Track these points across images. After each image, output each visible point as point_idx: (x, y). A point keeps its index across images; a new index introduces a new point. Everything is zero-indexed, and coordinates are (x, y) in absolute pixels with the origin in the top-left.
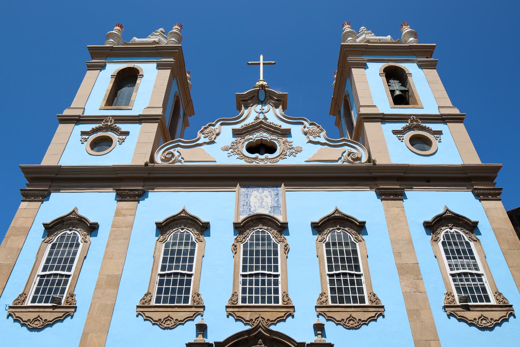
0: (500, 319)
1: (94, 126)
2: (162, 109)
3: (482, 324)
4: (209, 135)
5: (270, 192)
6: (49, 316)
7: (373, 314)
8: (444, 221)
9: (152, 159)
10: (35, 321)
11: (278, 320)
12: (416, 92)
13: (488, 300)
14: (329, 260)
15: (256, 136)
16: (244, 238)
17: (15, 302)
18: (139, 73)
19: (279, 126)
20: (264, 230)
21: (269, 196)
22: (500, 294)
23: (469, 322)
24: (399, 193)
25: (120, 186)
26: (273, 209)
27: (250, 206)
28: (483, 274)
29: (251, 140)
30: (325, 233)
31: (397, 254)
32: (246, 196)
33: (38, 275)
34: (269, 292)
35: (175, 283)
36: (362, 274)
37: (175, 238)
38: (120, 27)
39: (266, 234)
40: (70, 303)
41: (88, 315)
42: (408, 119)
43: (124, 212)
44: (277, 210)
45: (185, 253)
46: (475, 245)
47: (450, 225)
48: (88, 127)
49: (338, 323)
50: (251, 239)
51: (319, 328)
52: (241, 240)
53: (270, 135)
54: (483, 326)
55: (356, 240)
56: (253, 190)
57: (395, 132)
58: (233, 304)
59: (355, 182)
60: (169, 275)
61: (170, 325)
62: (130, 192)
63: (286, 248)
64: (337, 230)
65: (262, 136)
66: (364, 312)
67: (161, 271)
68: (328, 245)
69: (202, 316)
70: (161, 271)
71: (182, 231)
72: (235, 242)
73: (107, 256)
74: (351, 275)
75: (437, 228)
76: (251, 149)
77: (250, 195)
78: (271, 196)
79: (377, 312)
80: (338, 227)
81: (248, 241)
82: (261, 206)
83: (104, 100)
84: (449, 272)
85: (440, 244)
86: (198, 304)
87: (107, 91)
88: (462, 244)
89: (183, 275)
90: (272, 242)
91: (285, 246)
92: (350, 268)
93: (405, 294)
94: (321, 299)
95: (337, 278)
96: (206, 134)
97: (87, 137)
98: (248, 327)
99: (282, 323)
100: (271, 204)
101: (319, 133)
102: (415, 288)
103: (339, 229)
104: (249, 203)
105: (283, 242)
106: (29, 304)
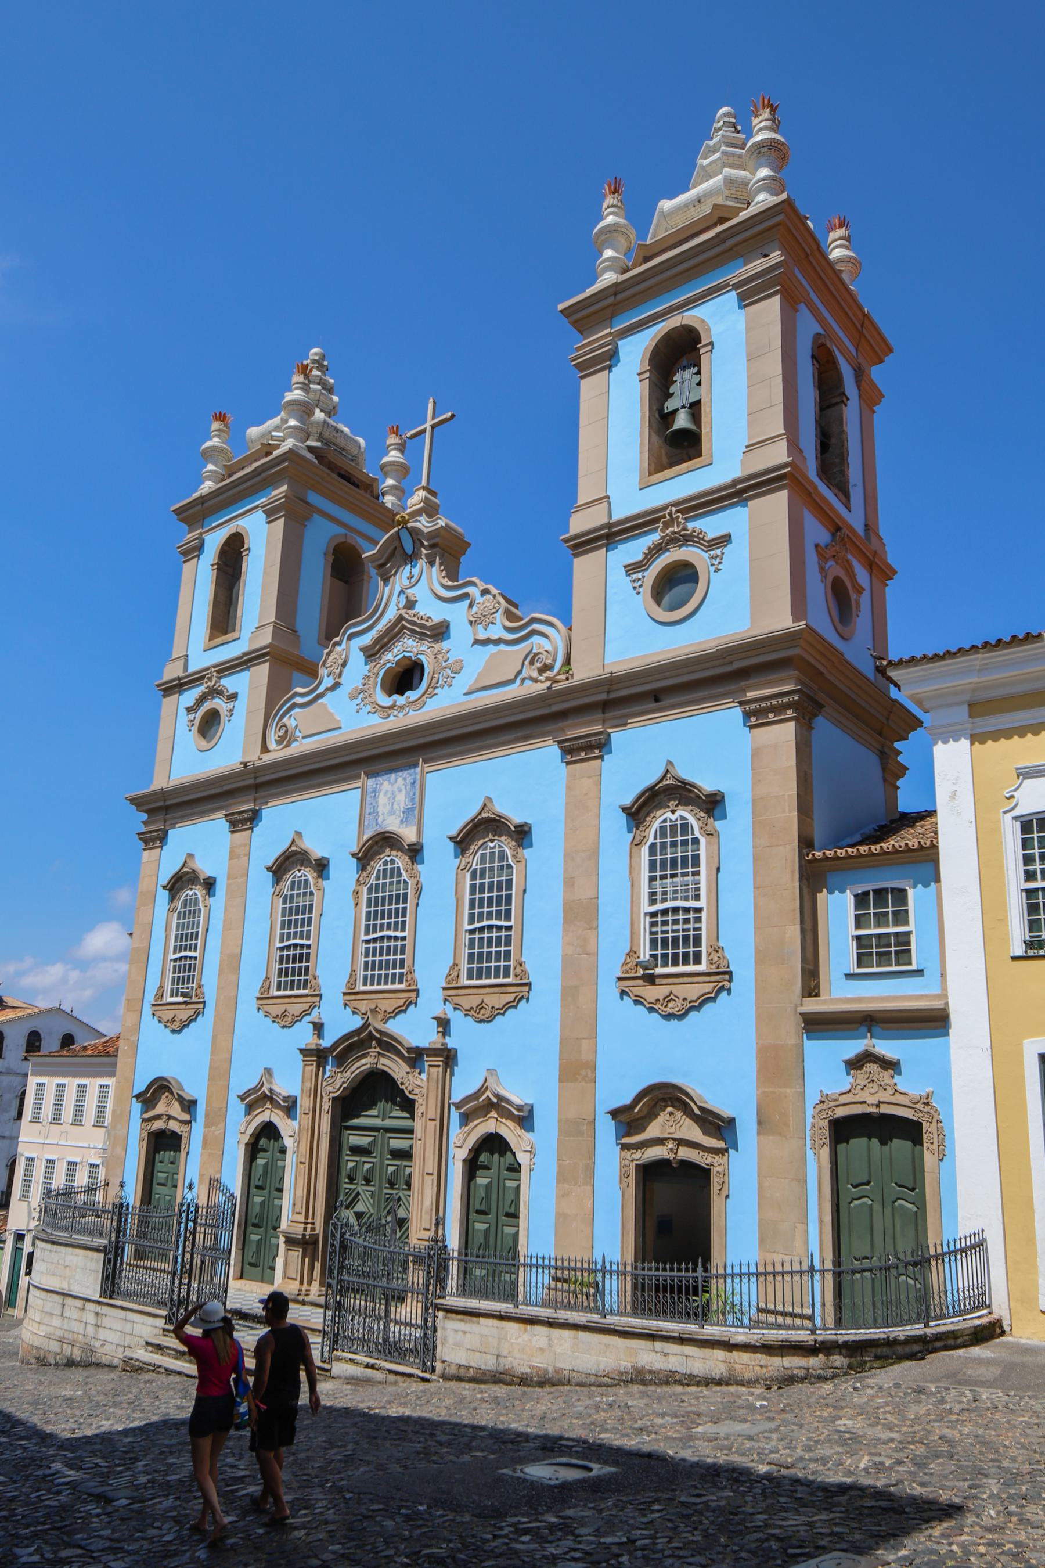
7: (511, 997)
8: (662, 796)
24: (594, 743)
31: (569, 882)
47: (672, 804)
51: (444, 1024)
59: (527, 732)
75: (647, 815)
80: (491, 836)
85: (645, 850)
93: (565, 957)
103: (492, 841)
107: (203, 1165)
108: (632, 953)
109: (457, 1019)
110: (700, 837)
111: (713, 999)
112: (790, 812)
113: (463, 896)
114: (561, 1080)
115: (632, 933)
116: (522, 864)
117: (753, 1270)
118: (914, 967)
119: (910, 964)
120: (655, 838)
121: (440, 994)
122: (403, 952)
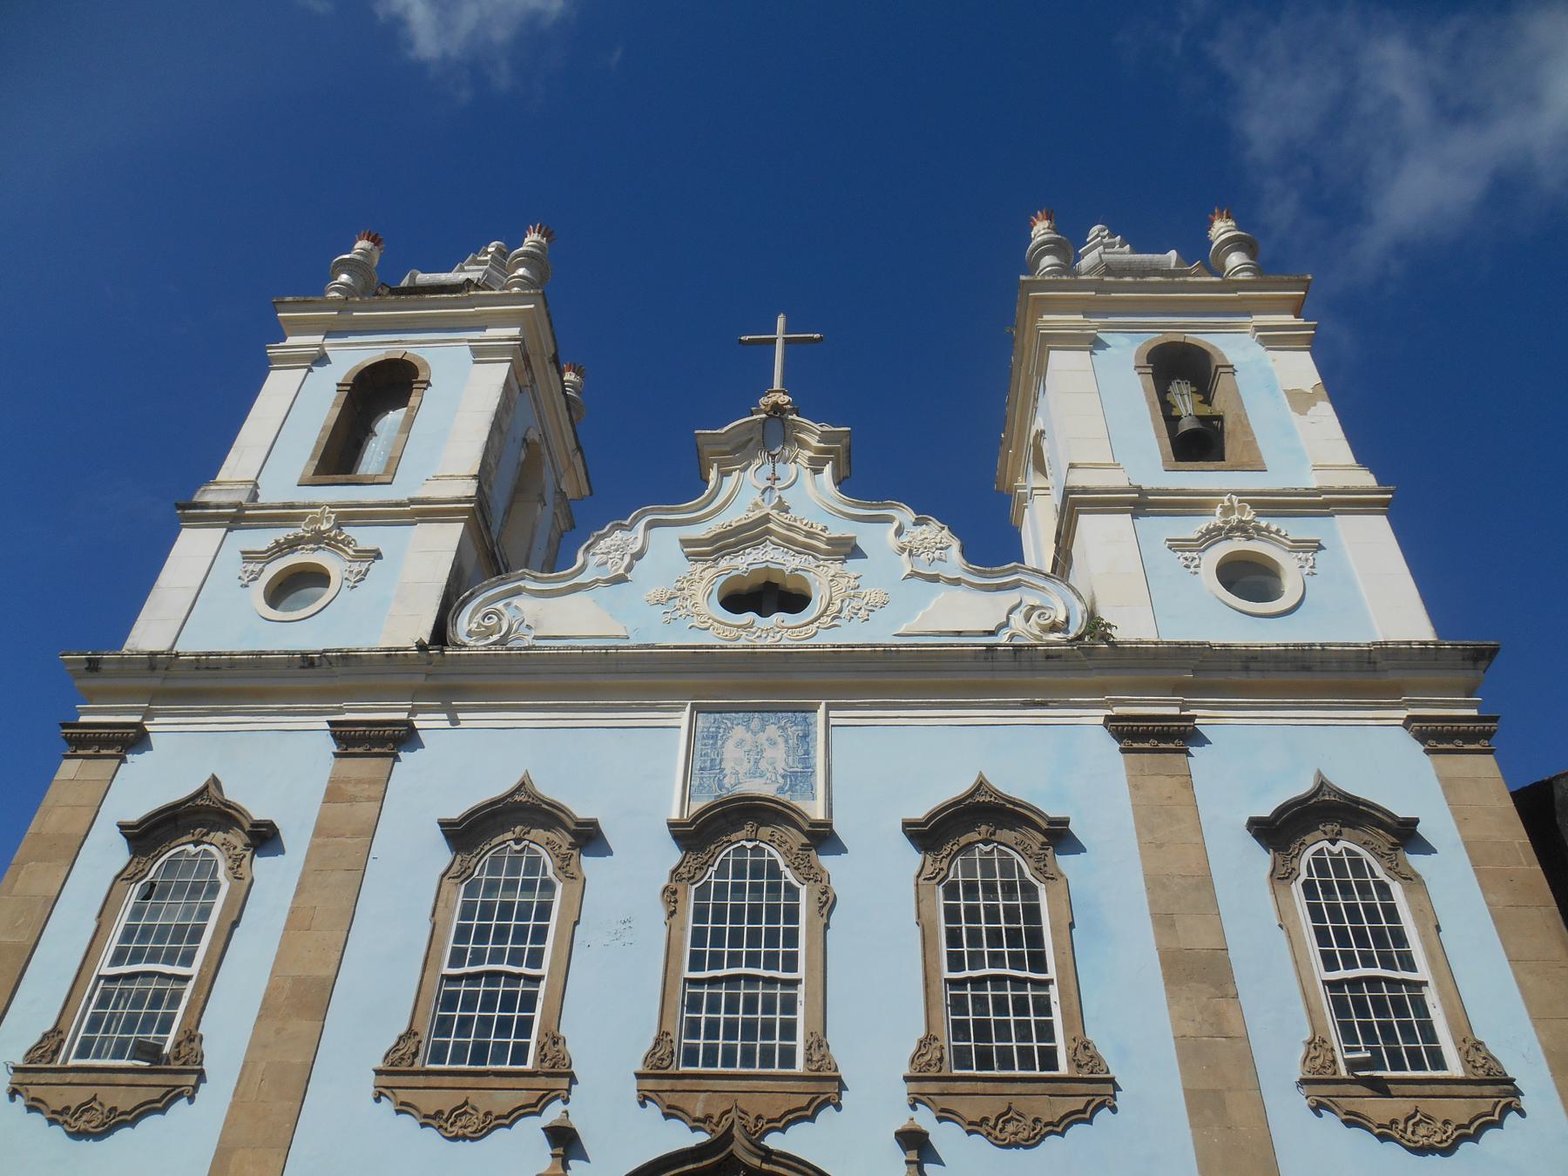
0: (1471, 1122)
1: (282, 534)
2: (474, 483)
3: (1416, 1139)
4: (611, 556)
5: (783, 728)
6: (124, 1100)
7: (1079, 1103)
9: (440, 634)
10: (83, 1112)
11: (790, 1117)
12: (1245, 422)
13: (1438, 1061)
14: (953, 938)
15: (745, 563)
16: (701, 868)
17: (31, 1055)
18: (417, 375)
19: (820, 528)
20: (762, 845)
21: (780, 740)
22: (1478, 1046)
23: (1377, 1131)
25: (340, 711)
26: (791, 781)
27: (722, 770)
28: (1425, 984)
29: (735, 573)
30: (945, 853)
31: (1163, 920)
32: (711, 742)
33: (99, 977)
34: (768, 1032)
35: (489, 1003)
36: (1052, 980)
37: (495, 866)
38: (371, 241)
39: (766, 858)
40: (183, 1060)
41: (234, 1096)
42: (1212, 505)
43: (351, 789)
44: (801, 784)
45: (524, 914)
46: (1407, 891)
48: (262, 539)
49: (973, 1128)
50: (721, 872)
52: (690, 875)
53: (794, 556)
54: (1418, 1145)
55: (1037, 874)
56: (732, 724)
57: (1177, 545)
58: (658, 1068)
60: (474, 978)
61: (469, 1129)
62: (371, 731)
63: (824, 899)
64: (980, 845)
65: (768, 558)
66: (1050, 1095)
67: (451, 965)
68: (951, 892)
69: (566, 1101)
70: (451, 965)
71: (518, 848)
72: (671, 881)
73: (298, 921)
74: (1019, 983)
76: (737, 600)
77: (724, 737)
78: (786, 741)
79: (1091, 1098)
81: (710, 877)
82: (755, 773)
83: (313, 457)
84: (1321, 974)
85: (1297, 889)
86: (553, 1067)
87: (322, 430)
88: (1364, 889)
89: (513, 978)
90: (783, 880)
91: (823, 893)
92: (1017, 961)
93: (1180, 1039)
94: (923, 1055)
95: (973, 993)
96: (603, 553)
97: (258, 567)
98: (702, 1137)
99: (805, 1125)
100: (783, 765)
101: (941, 549)
102: (1212, 1025)
103: (986, 842)
104: (718, 761)
105: (816, 881)
106: (72, 1062)
108: (1317, 1043)
109: (945, 1137)
110: (1387, 880)
111: (1498, 1124)
115: (1310, 1011)
116: (1061, 884)
120: (1310, 873)
121: (903, 1090)
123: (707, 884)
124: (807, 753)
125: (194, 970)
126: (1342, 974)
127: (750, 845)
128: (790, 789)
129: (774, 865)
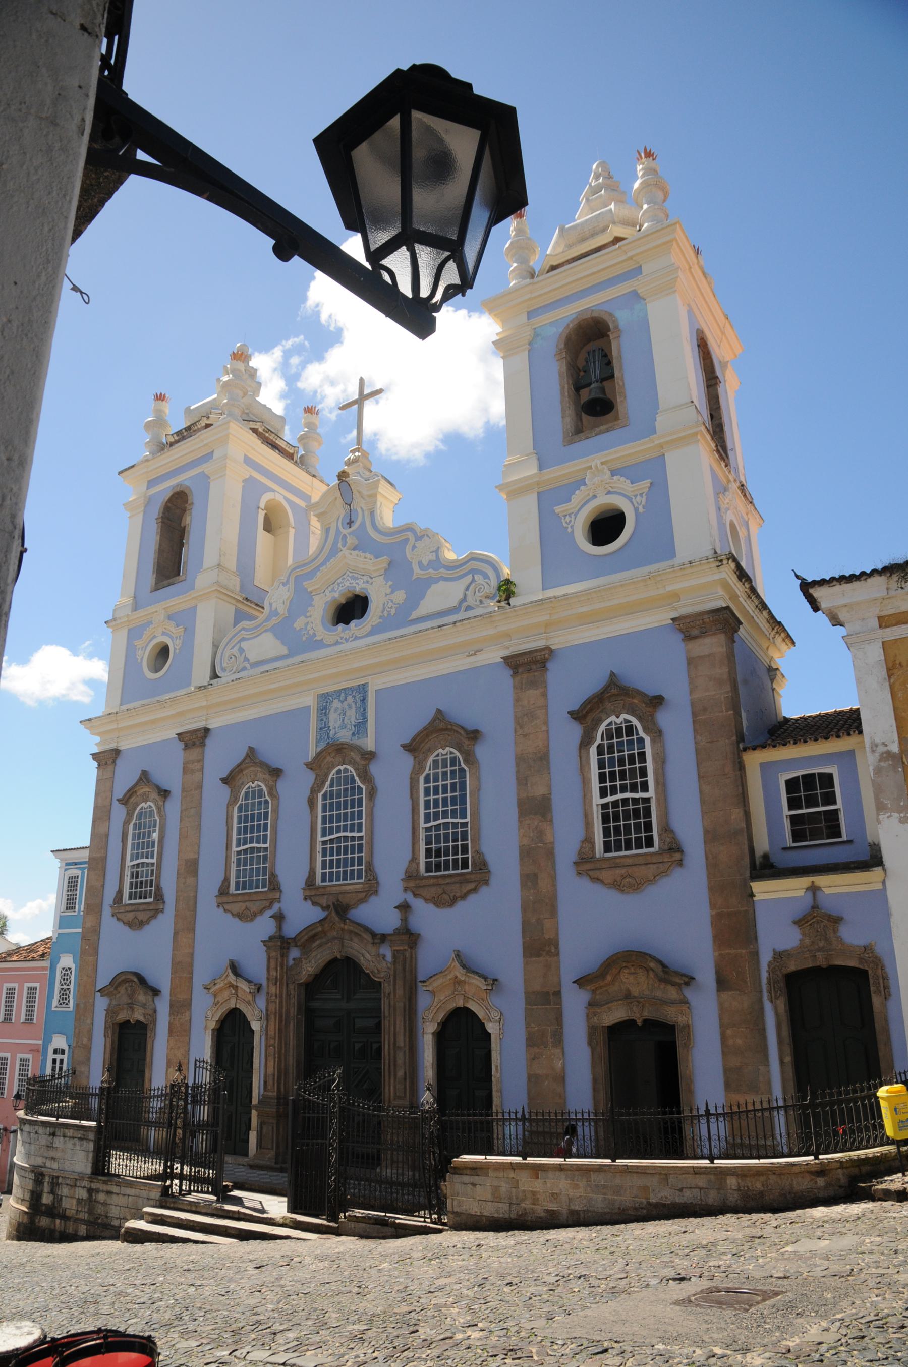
21: (353, 705)
27: (329, 727)
31: (522, 781)
46: (653, 741)
50: (331, 785)
69: (279, 902)
82: (343, 726)
85: (593, 750)
107: (170, 1049)
112: (727, 711)
113: (418, 798)
114: (525, 956)
117: (720, 1111)
118: (844, 838)
119: (840, 836)
120: (602, 739)
121: (400, 886)
122: (360, 851)
123: (326, 791)
124: (364, 710)
125: (154, 861)
126: (609, 799)
127: (342, 768)
128: (357, 733)
129: (353, 776)
